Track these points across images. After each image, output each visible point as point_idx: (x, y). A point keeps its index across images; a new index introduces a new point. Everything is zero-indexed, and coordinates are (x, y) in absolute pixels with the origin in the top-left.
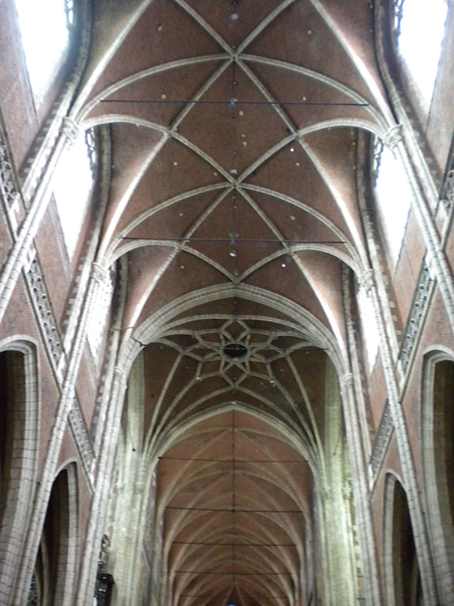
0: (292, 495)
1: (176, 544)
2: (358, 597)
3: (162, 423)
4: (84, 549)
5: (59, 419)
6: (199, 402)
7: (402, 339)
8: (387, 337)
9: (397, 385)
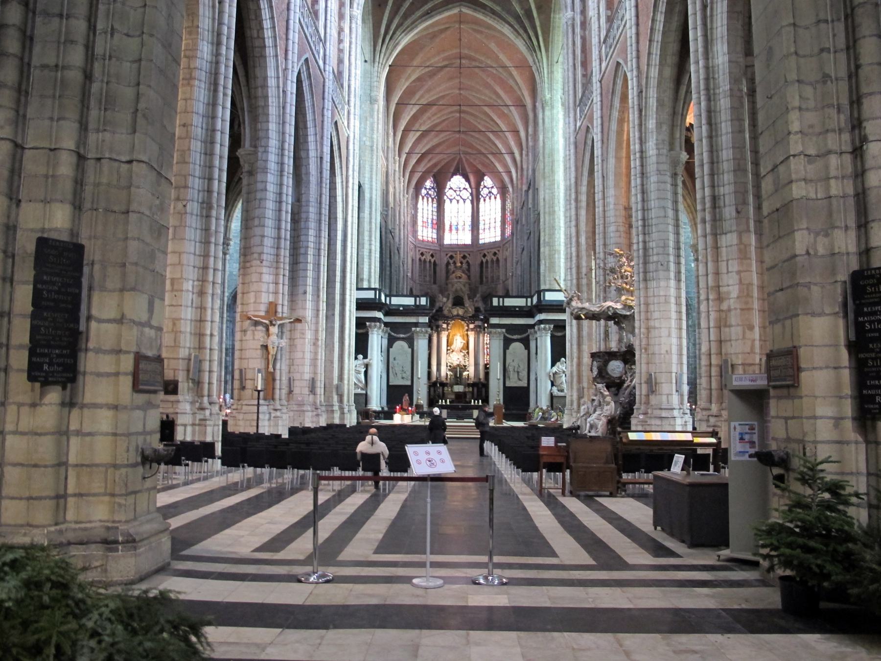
0: (516, 88)
1: (406, 131)
3: (391, 33)
4: (347, 182)
5: (326, 101)
6: (426, 7)
7: (610, 20)
8: (599, 14)
9: (600, 64)
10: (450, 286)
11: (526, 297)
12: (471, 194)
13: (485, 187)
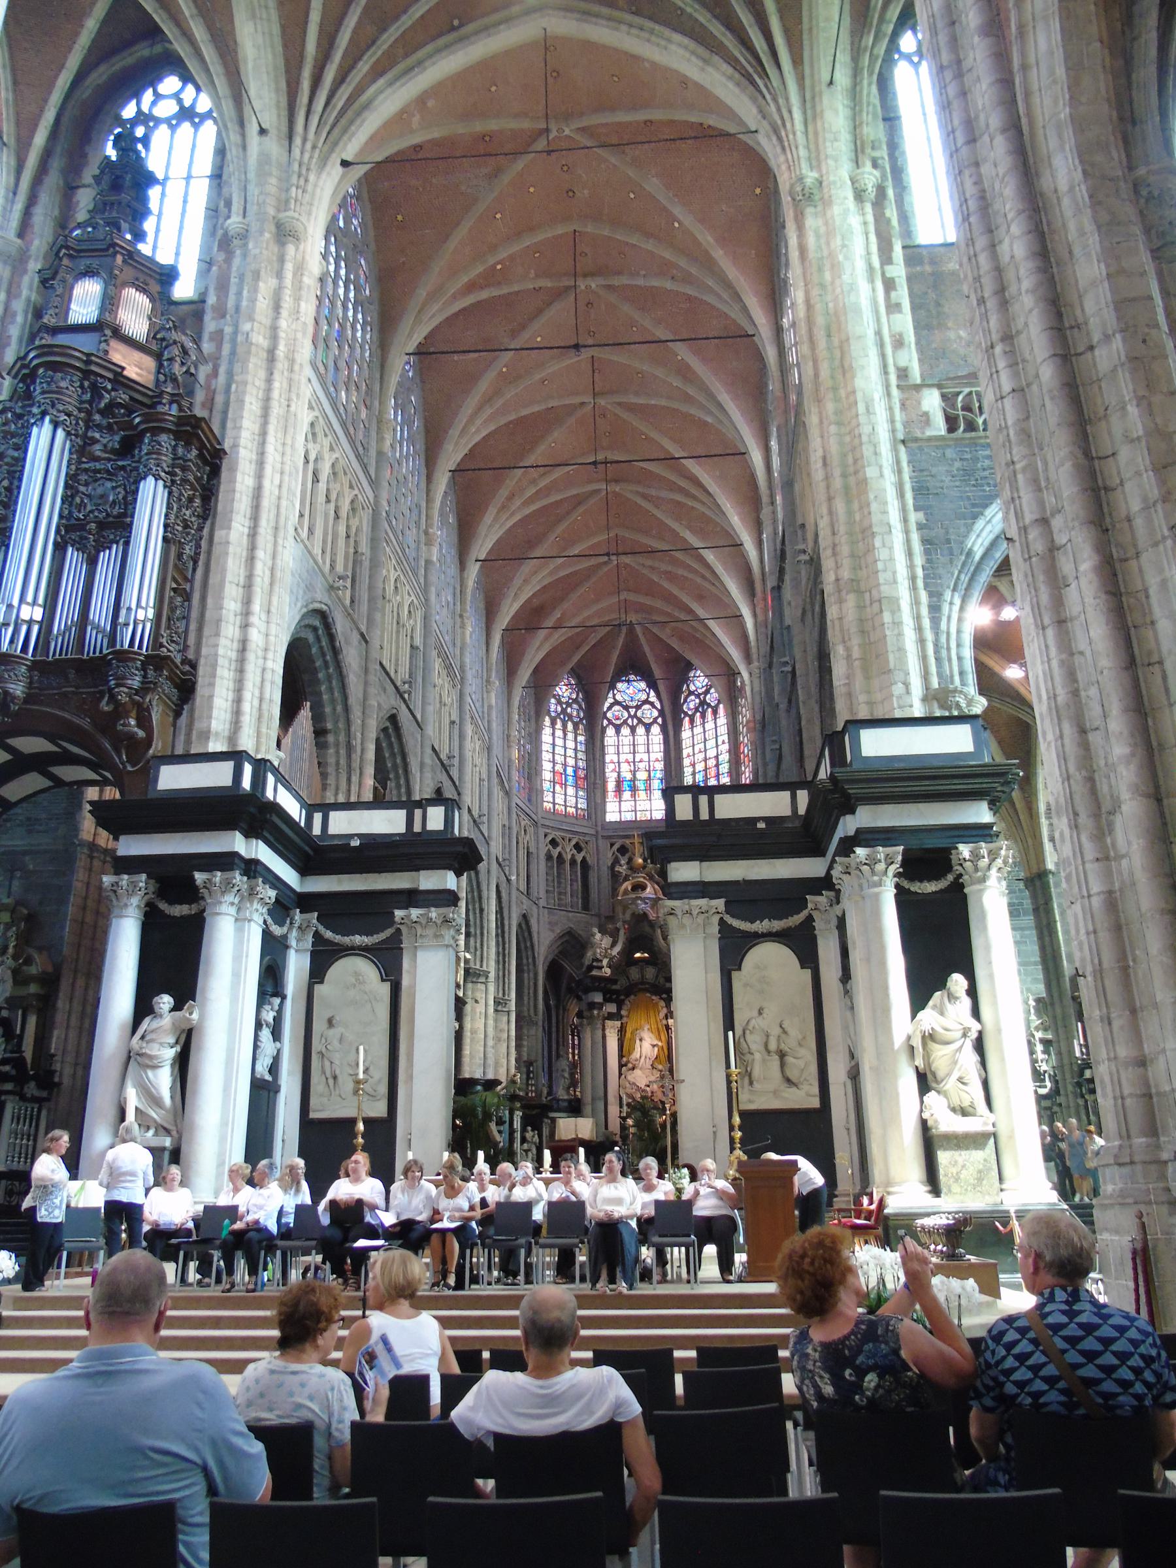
2: (900, 436)
10: (619, 909)
11: (792, 787)
12: (662, 713)
13: (691, 693)
